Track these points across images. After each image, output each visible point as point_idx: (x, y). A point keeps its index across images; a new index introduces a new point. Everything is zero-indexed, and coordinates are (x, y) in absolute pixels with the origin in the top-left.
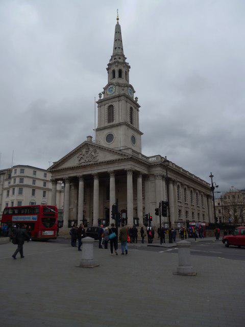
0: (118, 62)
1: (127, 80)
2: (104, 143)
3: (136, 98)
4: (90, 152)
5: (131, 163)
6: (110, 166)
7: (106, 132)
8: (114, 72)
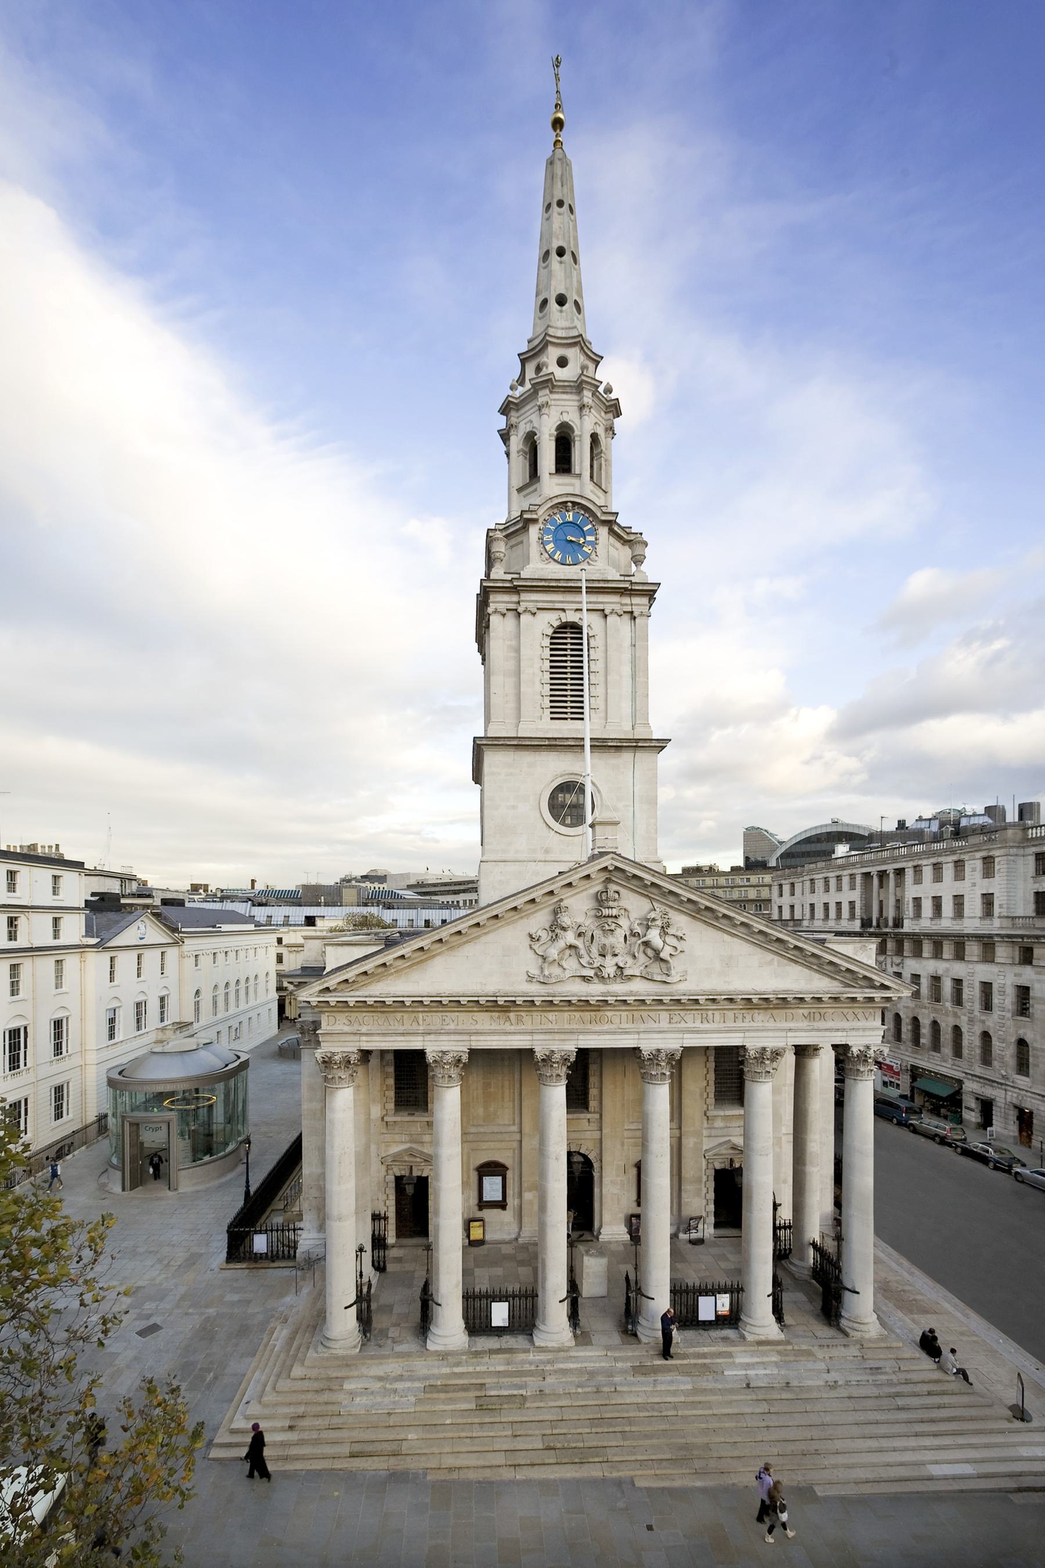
6: (761, 1019)
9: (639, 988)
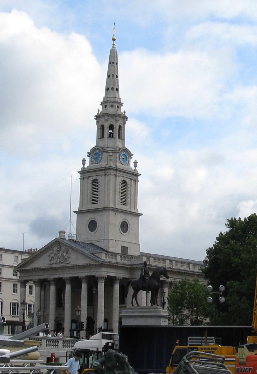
0: (109, 115)
1: (121, 136)
3: (136, 163)
4: (61, 252)
5: (103, 269)
7: (90, 217)
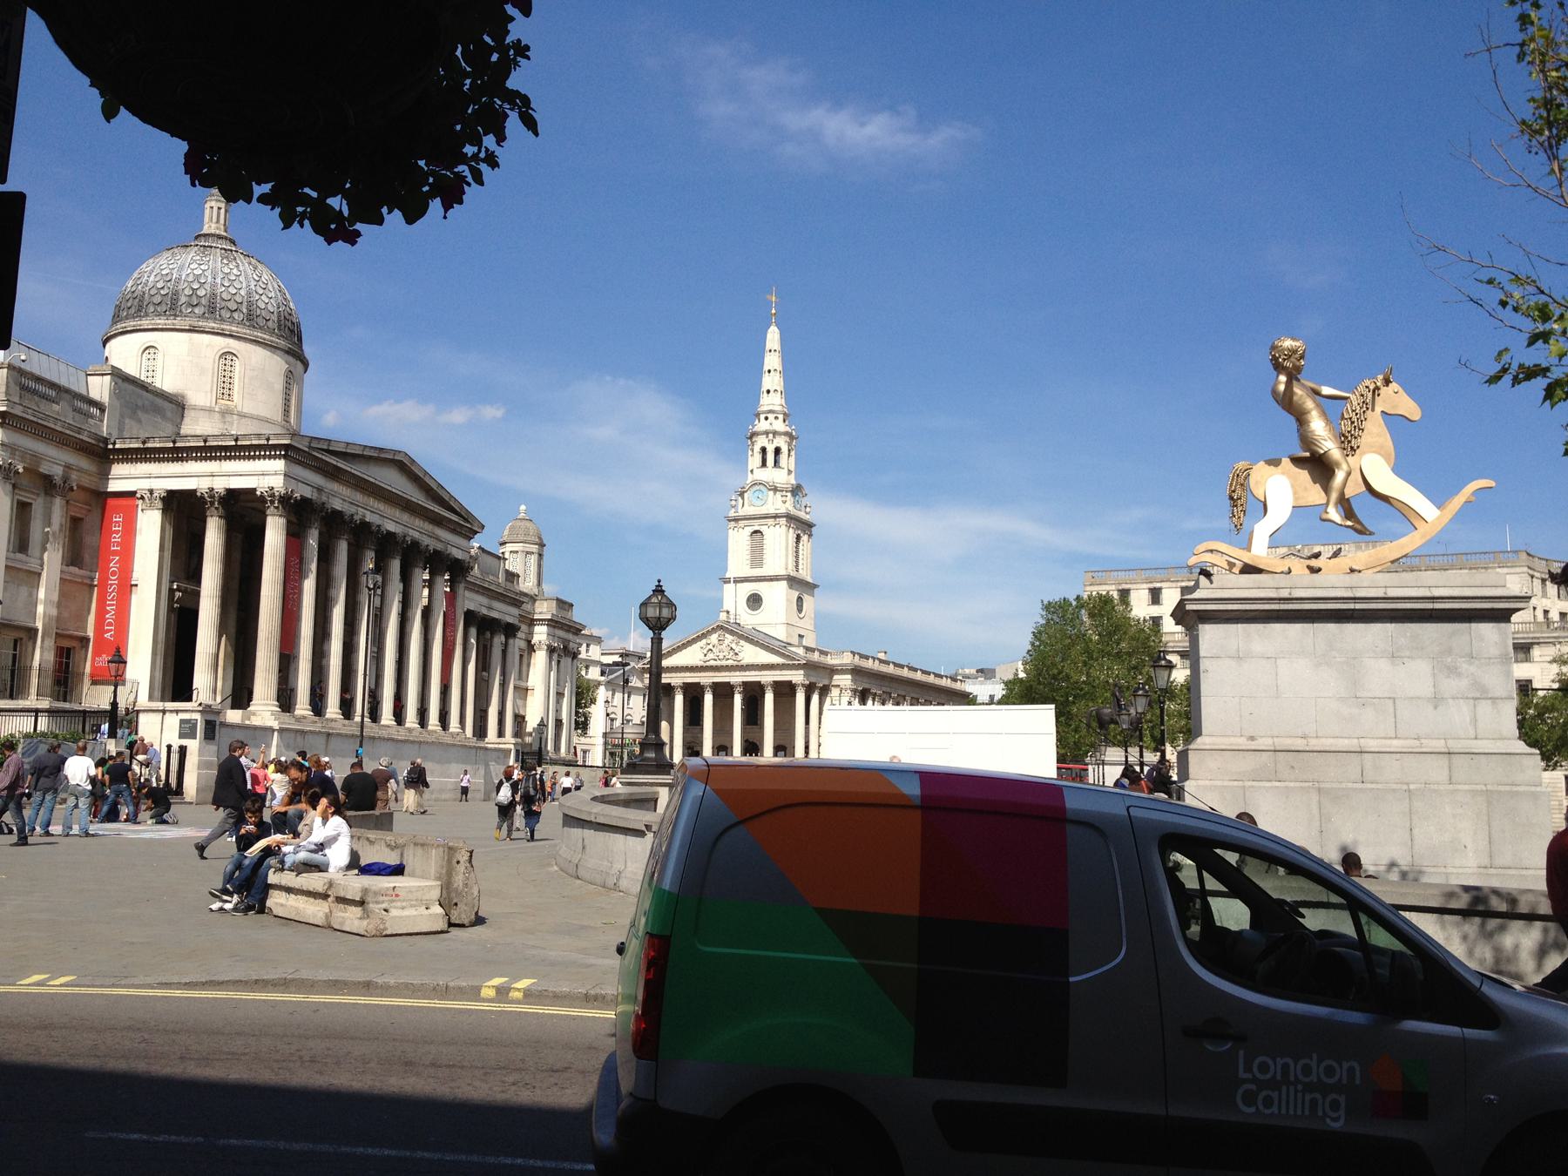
0: (775, 433)
2: (748, 619)
7: (747, 589)
8: (764, 450)
9: (730, 662)
